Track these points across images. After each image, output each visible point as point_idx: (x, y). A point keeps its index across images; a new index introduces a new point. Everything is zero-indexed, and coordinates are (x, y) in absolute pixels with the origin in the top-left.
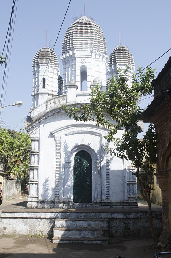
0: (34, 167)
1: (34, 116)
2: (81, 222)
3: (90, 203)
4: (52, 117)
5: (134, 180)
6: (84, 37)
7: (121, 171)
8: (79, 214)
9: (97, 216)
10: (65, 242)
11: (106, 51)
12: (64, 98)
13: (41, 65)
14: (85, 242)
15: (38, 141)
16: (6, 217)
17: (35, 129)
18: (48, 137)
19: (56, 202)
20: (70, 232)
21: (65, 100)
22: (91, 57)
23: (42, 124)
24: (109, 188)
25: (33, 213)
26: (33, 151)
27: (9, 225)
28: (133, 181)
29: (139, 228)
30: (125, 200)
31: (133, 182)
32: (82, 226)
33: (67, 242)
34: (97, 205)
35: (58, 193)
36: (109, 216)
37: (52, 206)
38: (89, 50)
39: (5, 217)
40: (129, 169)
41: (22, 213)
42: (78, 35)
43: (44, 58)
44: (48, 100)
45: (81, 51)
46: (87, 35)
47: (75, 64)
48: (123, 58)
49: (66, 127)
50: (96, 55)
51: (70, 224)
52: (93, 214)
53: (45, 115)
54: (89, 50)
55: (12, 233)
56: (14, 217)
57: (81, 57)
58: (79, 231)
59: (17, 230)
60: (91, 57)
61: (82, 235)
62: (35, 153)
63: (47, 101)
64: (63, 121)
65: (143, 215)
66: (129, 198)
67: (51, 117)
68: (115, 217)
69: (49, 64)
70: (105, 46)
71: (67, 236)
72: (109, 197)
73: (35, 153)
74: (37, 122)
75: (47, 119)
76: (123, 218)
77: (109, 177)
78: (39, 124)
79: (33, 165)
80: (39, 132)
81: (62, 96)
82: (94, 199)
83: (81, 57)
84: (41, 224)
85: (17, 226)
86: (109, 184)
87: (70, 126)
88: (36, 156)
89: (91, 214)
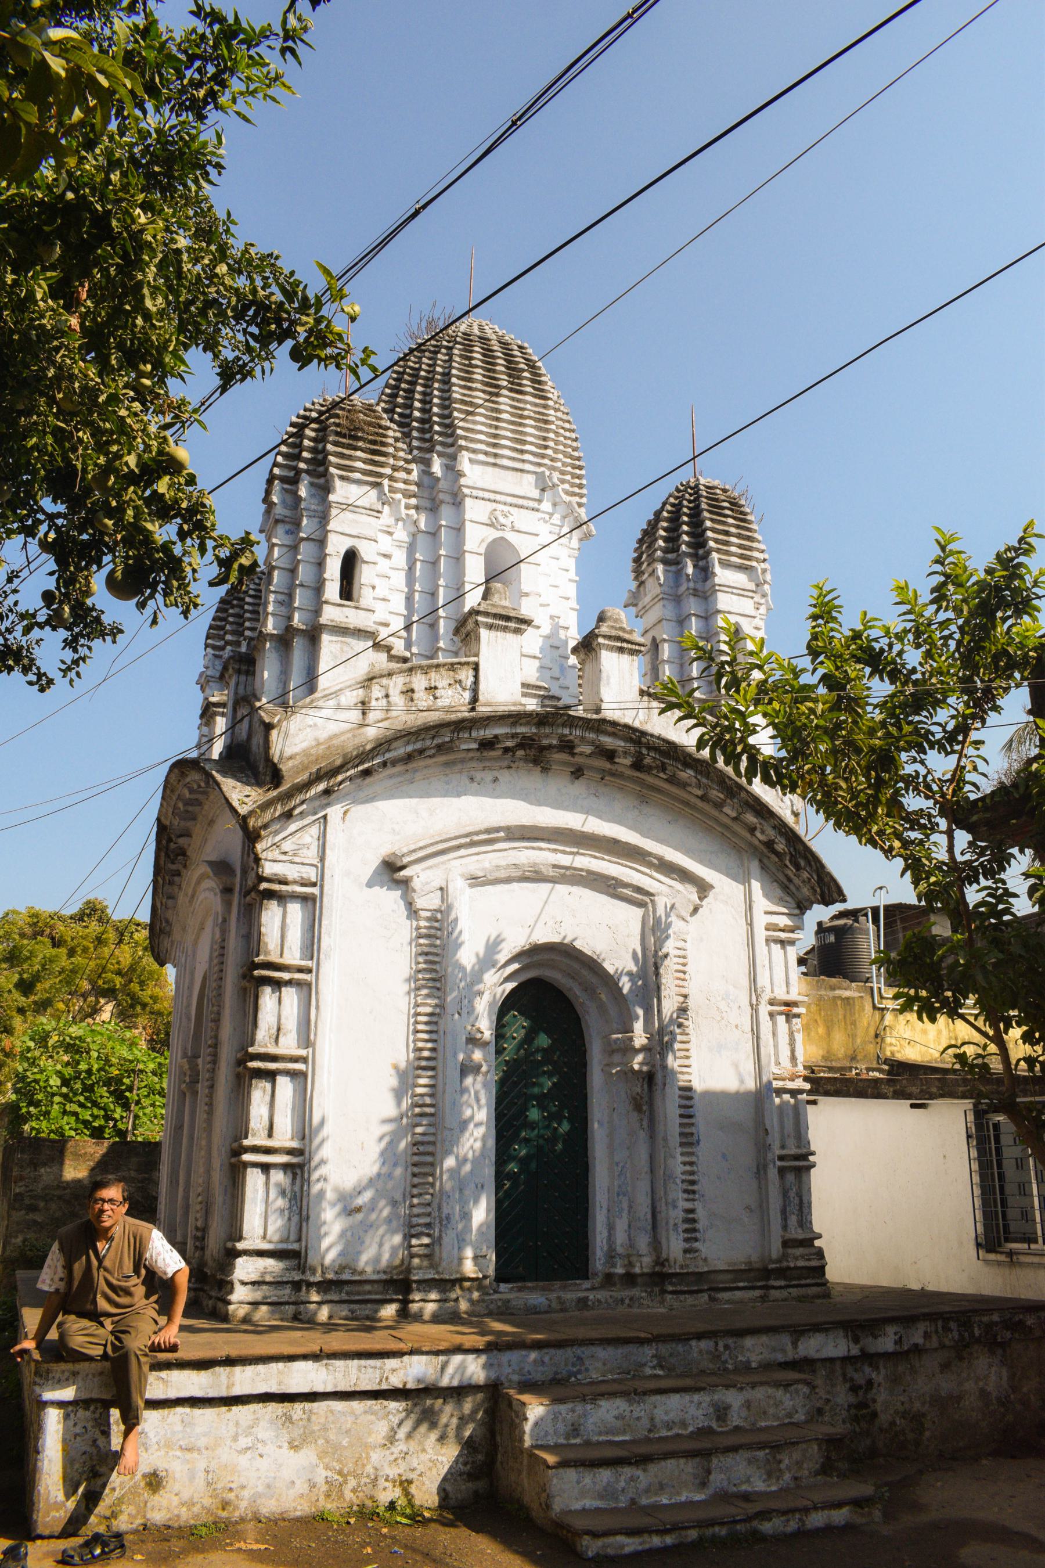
0: (274, 1058)
1: (288, 752)
2: (675, 1401)
3: (587, 1284)
5: (804, 1151)
6: (504, 401)
7: (748, 1093)
8: (631, 1348)
9: (726, 1356)
10: (656, 1541)
11: (584, 500)
12: (458, 677)
13: (342, 478)
14: (767, 1527)
15: (305, 899)
16: (173, 1394)
17: (293, 827)
18: (370, 884)
19: (418, 1282)
20: (645, 1470)
21: (464, 689)
22: (535, 505)
23: (338, 801)
24: (694, 1192)
25: (356, 1362)
26: (274, 958)
27: (188, 1455)
28: (799, 1151)
29: (917, 1405)
30: (774, 1255)
32: (684, 1424)
33: (669, 1540)
34: (636, 1292)
35: (428, 1225)
36: (783, 1351)
38: (528, 472)
40: (780, 1092)
41: (281, 1365)
42: (476, 389)
43: (360, 444)
45: (490, 469)
46: (518, 400)
47: (459, 530)
48: (739, 536)
49: (477, 833)
50: (555, 505)
51: (616, 1418)
52: (705, 1344)
54: (528, 472)
55: (208, 1511)
56: (224, 1393)
57: (492, 496)
58: (697, 1460)
59: (243, 1487)
60: (535, 505)
61: (718, 1479)
62: (286, 976)
63: (371, 679)
64: (454, 800)
65: (937, 1332)
66: (786, 1244)
67: (390, 771)
68: (812, 1354)
69: (386, 482)
70: (579, 477)
71: (633, 1501)
72: (696, 1245)
73: (286, 976)
74: (322, 786)
75: (369, 780)
76: (846, 1360)
77: (693, 1130)
79: (272, 1050)
81: (452, 664)
82: (611, 1255)
83: (491, 496)
85: (243, 1460)
86: (695, 1168)
87: (502, 834)
88: (290, 995)
89: (693, 1343)
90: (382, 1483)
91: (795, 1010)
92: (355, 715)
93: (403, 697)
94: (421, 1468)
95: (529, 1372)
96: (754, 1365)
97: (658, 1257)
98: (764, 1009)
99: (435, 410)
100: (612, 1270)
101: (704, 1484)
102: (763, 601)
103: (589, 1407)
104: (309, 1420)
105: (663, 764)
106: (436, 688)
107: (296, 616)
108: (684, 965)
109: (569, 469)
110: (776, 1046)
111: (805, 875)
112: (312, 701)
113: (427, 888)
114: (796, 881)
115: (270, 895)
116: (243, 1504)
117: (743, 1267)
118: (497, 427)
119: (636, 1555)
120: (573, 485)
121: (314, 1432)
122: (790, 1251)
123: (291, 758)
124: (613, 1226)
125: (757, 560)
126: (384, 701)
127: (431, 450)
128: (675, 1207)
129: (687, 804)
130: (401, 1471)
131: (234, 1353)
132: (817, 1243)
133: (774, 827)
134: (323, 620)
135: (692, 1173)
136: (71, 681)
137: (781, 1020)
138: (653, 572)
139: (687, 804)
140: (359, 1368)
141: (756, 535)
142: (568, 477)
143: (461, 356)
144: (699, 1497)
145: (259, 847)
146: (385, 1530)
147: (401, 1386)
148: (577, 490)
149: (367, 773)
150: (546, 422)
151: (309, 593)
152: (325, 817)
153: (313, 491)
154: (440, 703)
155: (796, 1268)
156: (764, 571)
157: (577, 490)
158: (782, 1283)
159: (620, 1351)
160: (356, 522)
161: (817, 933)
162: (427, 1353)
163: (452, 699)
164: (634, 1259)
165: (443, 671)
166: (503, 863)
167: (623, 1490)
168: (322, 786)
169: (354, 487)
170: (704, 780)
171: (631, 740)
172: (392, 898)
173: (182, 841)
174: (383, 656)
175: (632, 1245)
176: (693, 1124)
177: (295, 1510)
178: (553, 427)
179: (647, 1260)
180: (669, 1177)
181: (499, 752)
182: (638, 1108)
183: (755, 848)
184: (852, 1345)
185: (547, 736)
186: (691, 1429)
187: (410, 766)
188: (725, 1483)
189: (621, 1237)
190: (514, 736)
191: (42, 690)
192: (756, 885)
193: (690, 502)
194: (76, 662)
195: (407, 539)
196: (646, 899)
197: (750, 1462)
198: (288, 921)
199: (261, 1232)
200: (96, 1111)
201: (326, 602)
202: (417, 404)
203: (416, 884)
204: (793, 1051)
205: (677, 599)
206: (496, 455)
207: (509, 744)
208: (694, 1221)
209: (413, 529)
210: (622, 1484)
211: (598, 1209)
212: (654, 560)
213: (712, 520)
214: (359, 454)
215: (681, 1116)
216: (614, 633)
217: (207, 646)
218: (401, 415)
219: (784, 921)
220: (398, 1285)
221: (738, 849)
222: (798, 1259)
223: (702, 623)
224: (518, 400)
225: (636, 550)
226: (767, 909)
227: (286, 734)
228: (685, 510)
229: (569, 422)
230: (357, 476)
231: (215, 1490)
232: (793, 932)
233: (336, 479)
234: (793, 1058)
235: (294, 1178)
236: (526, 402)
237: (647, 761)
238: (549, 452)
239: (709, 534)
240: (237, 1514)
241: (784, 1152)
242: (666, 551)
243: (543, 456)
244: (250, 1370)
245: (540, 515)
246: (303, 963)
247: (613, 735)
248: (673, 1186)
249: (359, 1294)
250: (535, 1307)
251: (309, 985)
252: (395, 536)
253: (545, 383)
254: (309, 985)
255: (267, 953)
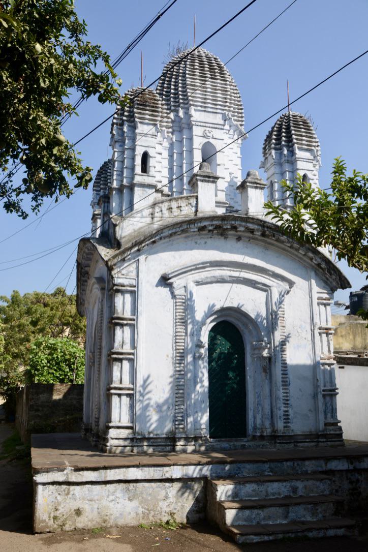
1: (123, 235)
2: (276, 485)
3: (245, 439)
4: (167, 240)
5: (333, 388)
7: (310, 366)
9: (298, 468)
10: (266, 538)
11: (243, 123)
12: (190, 202)
13: (141, 123)
14: (310, 535)
16: (84, 480)
17: (126, 265)
18: (157, 286)
20: (263, 511)
21: (192, 207)
22: (222, 127)
24: (288, 404)
25: (153, 468)
26: (120, 315)
27: (91, 503)
28: (331, 388)
30: (321, 429)
31: (331, 390)
32: (280, 494)
33: (271, 538)
34: (264, 443)
36: (321, 467)
37: (168, 448)
38: (219, 113)
39: (79, 480)
40: (323, 364)
41: (124, 469)
42: (196, 79)
44: (157, 201)
45: (203, 113)
46: (214, 83)
47: (191, 139)
48: (306, 137)
49: (199, 264)
50: (230, 126)
52: (288, 463)
53: (155, 233)
54: (219, 113)
56: (103, 480)
57: (204, 124)
58: (284, 508)
59: (111, 515)
60: (222, 127)
61: (292, 515)
62: (125, 322)
66: (326, 424)
67: (163, 241)
68: (333, 468)
69: (158, 123)
70: (241, 113)
71: (258, 523)
72: (289, 424)
73: (125, 322)
74: (136, 248)
75: (155, 245)
76: (347, 471)
77: (287, 380)
78: (137, 254)
79: (120, 350)
80: (134, 273)
81: (187, 197)
82: (255, 428)
83: (204, 124)
84: (170, 495)
85: (111, 505)
87: (208, 264)
88: (127, 330)
89: (285, 463)
90: (163, 514)
91: (330, 332)
92: (149, 220)
93: (168, 211)
94: (178, 508)
95: (219, 473)
96: (309, 472)
97: (274, 429)
98: (317, 332)
99: (180, 89)
100: (255, 434)
101: (286, 517)
102: (317, 163)
103: (242, 486)
104: (136, 490)
105: (274, 234)
106: (181, 207)
107: (125, 180)
108: (283, 314)
109: (237, 110)
110: (322, 346)
111: (334, 277)
112: (132, 215)
113: (179, 287)
114: (331, 280)
115: (118, 291)
116: (112, 521)
117: (308, 434)
118: (205, 95)
119: (258, 543)
120: (238, 117)
121: (137, 494)
122: (328, 427)
123: (124, 237)
124: (255, 417)
125: (315, 146)
126: (160, 213)
127: (179, 106)
128: (280, 410)
129: (284, 249)
130: (171, 509)
131: (107, 465)
132: (339, 424)
133: (321, 258)
134: (135, 182)
135: (287, 396)
136: (36, 213)
137: (324, 335)
138: (270, 154)
139: (284, 249)
140: (154, 471)
141: (314, 136)
142: (236, 114)
143: (190, 65)
144: (284, 522)
145: (113, 273)
146: (164, 531)
147: (170, 477)
148: (240, 119)
149: (154, 242)
150: (226, 91)
151: (130, 170)
152: (138, 260)
153: (130, 128)
154: (183, 213)
155: (330, 434)
156: (317, 151)
157: (240, 119)
158: (325, 440)
159: (255, 465)
160: (147, 141)
161: (350, 297)
162: (180, 465)
163: (187, 211)
164: (264, 430)
165: (184, 200)
166: (209, 276)
167: (254, 518)
168: (136, 248)
169: (145, 126)
170: (291, 240)
171: (260, 225)
172: (165, 291)
173: (86, 269)
174: (159, 195)
175: (263, 425)
176: (287, 378)
177: (131, 523)
178: (229, 93)
179: (269, 430)
180: (277, 398)
181: (207, 232)
182: (265, 371)
183: (313, 267)
184: (350, 465)
185: (226, 225)
186: (282, 496)
187: (171, 239)
188: (295, 517)
189: (259, 421)
190: (212, 225)
191: (24, 218)
192: (313, 282)
193: (286, 123)
194: (37, 206)
195: (168, 146)
196: (268, 288)
197: (305, 509)
198: (125, 301)
199: (119, 420)
200: (60, 372)
201: (136, 174)
202: (172, 87)
203: (175, 285)
204: (329, 348)
205: (281, 165)
206: (205, 107)
207: (211, 228)
208: (288, 415)
209: (171, 142)
210: (254, 516)
211: (250, 410)
212: (271, 149)
213: (295, 130)
214: (147, 112)
215: (282, 374)
216: (253, 181)
217: (94, 190)
218: (166, 92)
219: (325, 296)
220: (172, 440)
221: (305, 267)
222: (331, 431)
223: (291, 174)
224: (214, 83)
225: (264, 144)
226: (318, 291)
227: (122, 228)
228: (284, 127)
229: (236, 90)
230: (147, 121)
231: (101, 515)
232: (329, 300)
233: (138, 123)
234: (329, 351)
235: (130, 399)
236: (217, 83)
237: (267, 233)
238: (227, 104)
239: (294, 136)
240: (109, 525)
241: (325, 388)
242: (276, 144)
243: (225, 106)
244: (113, 471)
245: (224, 131)
246: (132, 317)
247: (253, 223)
248: (280, 402)
249: (156, 442)
250: (224, 448)
251: (134, 325)
252: (163, 145)
253: (226, 74)
254: (134, 325)
255: (118, 313)
